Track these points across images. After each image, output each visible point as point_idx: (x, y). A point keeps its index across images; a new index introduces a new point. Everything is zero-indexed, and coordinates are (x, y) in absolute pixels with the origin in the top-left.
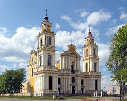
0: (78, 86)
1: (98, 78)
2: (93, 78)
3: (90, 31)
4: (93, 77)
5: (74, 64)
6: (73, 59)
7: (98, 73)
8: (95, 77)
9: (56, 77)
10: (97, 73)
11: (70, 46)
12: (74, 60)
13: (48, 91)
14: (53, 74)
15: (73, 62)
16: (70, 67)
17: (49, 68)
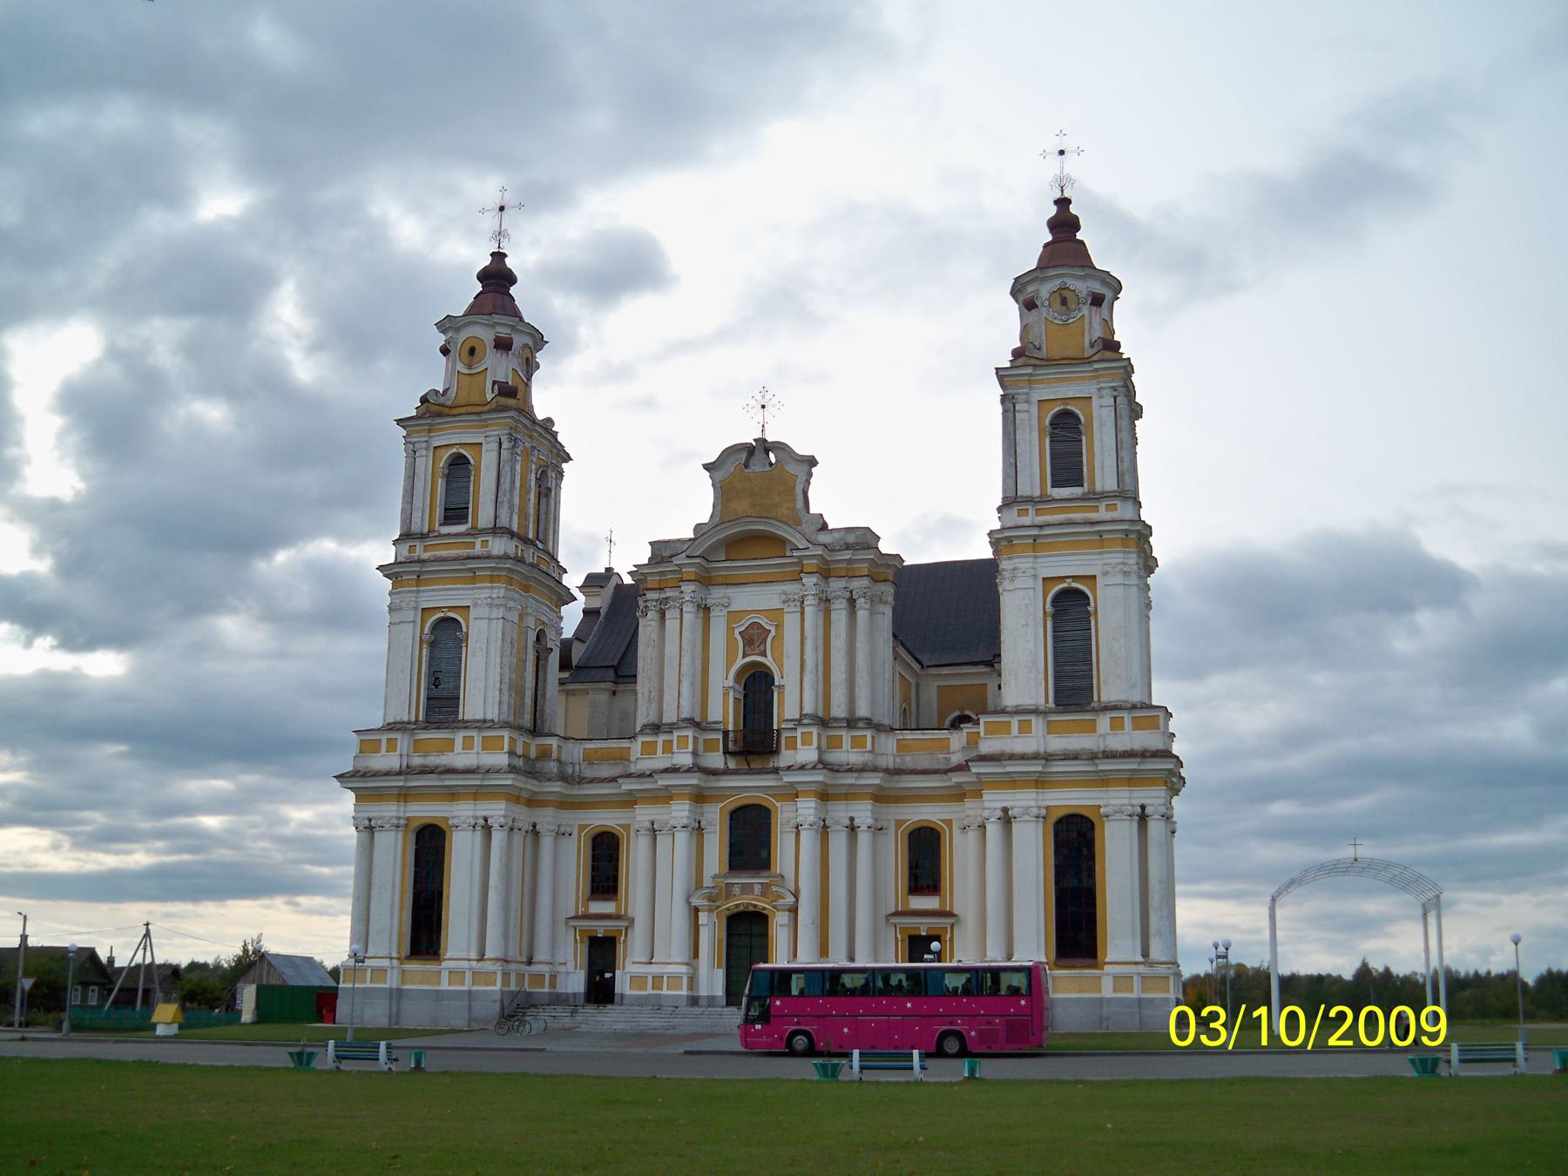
0: (794, 910)
1: (1103, 781)
2: (994, 800)
3: (1063, 203)
4: (1012, 782)
5: (768, 661)
6: (753, 600)
7: (1103, 722)
8: (1040, 782)
9: (487, 829)
10: (1091, 727)
11: (730, 467)
12: (776, 615)
13: (379, 972)
14: (452, 795)
15: (754, 638)
16: (723, 708)
17: (417, 746)
